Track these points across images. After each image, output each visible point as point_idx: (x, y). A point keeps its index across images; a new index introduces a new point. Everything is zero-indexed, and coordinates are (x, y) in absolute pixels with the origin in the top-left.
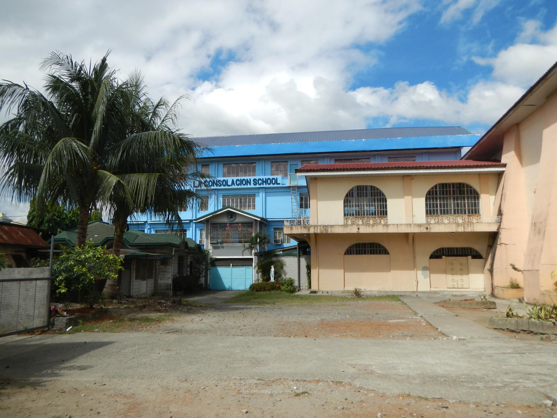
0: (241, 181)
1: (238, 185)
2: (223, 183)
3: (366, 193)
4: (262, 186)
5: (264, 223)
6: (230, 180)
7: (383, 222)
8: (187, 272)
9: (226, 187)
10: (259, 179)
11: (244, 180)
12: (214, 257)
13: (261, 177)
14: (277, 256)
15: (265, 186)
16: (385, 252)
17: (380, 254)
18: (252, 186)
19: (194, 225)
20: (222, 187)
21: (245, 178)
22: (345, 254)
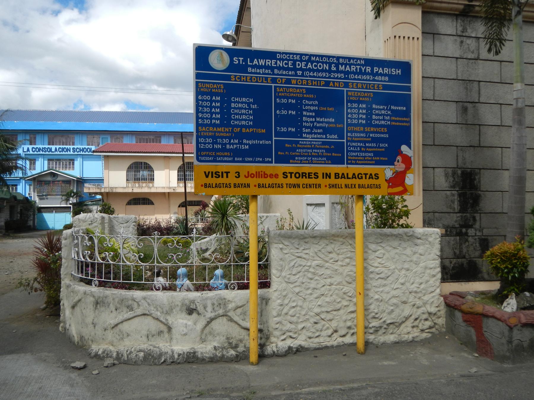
0: (63, 149)
1: (60, 152)
2: (48, 150)
3: (141, 167)
4: (79, 153)
5: (81, 182)
6: (53, 147)
7: (151, 185)
8: (18, 217)
9: (50, 153)
10: (77, 148)
11: (65, 148)
12: (39, 206)
13: (79, 147)
14: (86, 205)
15: (81, 153)
16: (150, 203)
17: (149, 204)
18: (72, 153)
19: (24, 181)
20: (47, 153)
21: (66, 147)
22: (127, 205)
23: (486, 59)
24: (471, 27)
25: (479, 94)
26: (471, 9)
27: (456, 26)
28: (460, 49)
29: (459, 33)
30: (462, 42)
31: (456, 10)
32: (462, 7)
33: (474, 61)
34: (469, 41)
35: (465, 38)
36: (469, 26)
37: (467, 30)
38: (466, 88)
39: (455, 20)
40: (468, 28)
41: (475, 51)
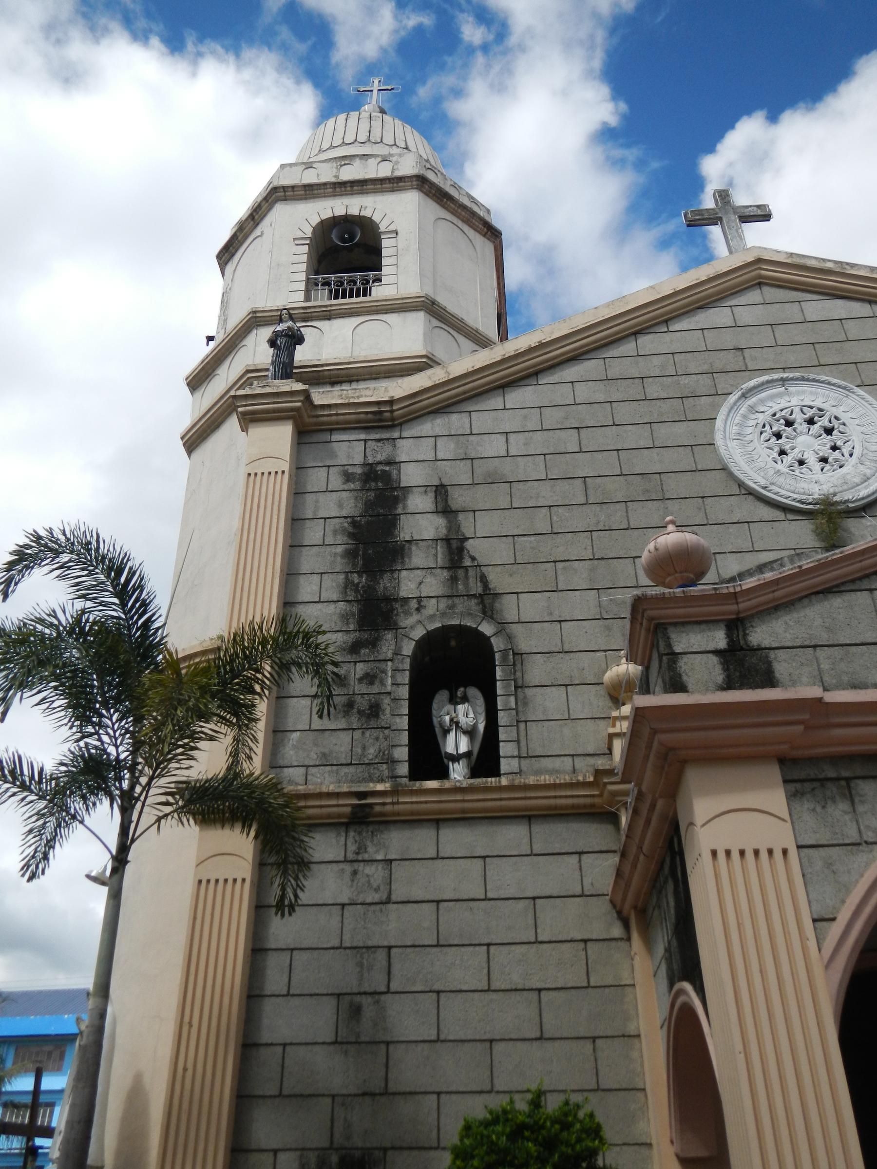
23: (406, 900)
24: (375, 842)
25: (389, 973)
26: (368, 810)
27: (346, 845)
28: (352, 886)
29: (350, 856)
30: (355, 873)
31: (339, 816)
32: (348, 810)
33: (378, 907)
34: (369, 870)
35: (362, 864)
36: (372, 841)
37: (366, 849)
38: (360, 965)
39: (343, 834)
40: (369, 843)
41: (382, 888)
